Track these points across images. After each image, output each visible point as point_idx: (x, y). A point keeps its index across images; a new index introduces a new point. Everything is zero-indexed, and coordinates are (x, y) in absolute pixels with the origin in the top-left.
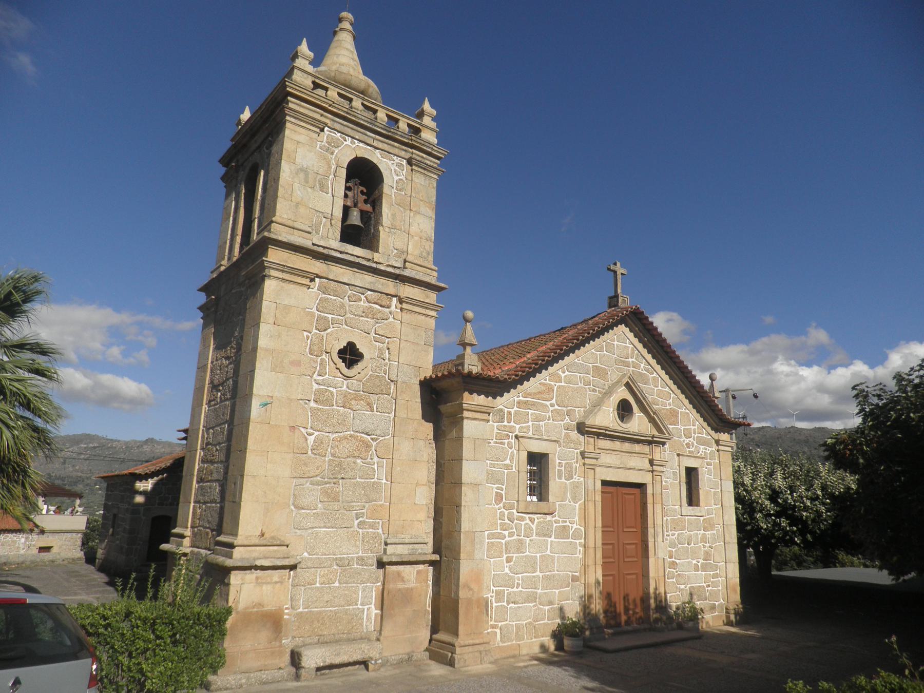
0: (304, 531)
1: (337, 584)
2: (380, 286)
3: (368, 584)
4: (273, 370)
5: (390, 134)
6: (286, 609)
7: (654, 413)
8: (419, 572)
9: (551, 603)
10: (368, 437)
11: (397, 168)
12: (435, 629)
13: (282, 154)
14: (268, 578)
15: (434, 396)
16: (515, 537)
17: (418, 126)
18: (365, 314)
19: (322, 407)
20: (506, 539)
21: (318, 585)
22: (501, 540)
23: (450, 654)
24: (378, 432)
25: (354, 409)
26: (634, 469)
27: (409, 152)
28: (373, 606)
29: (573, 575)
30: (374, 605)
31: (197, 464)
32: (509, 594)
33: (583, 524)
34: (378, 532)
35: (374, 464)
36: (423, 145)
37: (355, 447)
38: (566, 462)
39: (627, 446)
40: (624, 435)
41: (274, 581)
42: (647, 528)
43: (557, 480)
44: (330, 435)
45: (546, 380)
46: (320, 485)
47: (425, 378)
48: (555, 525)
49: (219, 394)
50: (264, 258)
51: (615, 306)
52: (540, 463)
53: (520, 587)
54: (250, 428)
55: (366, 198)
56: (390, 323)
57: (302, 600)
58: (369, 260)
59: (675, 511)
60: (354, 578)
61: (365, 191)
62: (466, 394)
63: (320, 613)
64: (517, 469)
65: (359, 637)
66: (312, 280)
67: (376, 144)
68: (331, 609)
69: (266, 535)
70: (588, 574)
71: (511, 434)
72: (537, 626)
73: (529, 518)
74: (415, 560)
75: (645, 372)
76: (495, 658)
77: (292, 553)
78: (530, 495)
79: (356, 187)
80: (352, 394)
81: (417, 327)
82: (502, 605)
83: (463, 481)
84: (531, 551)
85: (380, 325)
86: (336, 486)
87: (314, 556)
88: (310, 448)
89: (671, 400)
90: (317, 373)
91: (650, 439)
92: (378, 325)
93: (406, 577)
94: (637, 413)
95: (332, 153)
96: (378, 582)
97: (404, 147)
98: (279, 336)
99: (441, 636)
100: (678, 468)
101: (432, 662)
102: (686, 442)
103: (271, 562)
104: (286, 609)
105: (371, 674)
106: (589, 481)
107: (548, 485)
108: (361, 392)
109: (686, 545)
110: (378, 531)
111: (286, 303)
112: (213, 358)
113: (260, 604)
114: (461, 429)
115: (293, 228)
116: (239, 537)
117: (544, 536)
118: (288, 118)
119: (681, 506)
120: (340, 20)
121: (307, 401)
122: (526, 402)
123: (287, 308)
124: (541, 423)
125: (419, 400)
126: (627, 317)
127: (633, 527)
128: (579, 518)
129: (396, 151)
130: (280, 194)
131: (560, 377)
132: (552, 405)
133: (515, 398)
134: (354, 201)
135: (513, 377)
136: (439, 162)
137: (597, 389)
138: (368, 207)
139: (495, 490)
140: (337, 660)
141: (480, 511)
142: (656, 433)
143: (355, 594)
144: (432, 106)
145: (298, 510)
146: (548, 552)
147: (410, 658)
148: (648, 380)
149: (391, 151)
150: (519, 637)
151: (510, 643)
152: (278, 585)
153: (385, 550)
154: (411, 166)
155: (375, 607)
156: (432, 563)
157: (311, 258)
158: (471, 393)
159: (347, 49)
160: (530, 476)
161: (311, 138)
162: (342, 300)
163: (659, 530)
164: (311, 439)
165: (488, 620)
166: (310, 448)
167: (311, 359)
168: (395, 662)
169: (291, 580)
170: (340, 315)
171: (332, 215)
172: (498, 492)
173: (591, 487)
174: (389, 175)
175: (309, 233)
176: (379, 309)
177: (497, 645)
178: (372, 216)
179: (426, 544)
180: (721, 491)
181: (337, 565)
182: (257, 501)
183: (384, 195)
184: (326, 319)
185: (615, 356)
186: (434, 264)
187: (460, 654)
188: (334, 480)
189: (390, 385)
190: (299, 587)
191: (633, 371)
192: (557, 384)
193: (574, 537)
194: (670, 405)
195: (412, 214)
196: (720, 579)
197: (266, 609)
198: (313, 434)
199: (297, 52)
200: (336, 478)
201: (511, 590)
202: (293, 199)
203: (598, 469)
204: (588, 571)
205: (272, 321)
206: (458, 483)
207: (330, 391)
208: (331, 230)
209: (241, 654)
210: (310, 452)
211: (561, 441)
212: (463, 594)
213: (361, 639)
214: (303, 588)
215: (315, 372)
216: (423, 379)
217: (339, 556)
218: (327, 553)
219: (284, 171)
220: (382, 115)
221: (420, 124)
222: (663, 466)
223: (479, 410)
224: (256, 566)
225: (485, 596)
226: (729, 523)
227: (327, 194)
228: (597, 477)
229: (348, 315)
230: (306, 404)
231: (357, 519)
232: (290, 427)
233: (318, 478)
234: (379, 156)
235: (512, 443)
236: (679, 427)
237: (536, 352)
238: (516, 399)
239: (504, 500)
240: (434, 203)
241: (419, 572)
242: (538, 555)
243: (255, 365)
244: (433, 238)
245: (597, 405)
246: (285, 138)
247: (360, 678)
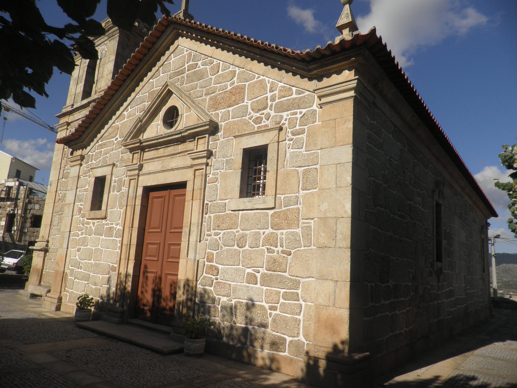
9: (95, 284)
16: (84, 236)
21: (53, 260)
22: (76, 237)
26: (173, 169)
29: (112, 266)
40: (159, 141)
45: (120, 124)
48: (105, 227)
75: (202, 67)
109: (236, 247)
117: (98, 235)
146: (99, 247)
151: (71, 304)
157: (68, 116)
192: (121, 122)
196: (301, 302)
201: (77, 270)
214: (49, 261)
223: (76, 159)
233: (60, 212)
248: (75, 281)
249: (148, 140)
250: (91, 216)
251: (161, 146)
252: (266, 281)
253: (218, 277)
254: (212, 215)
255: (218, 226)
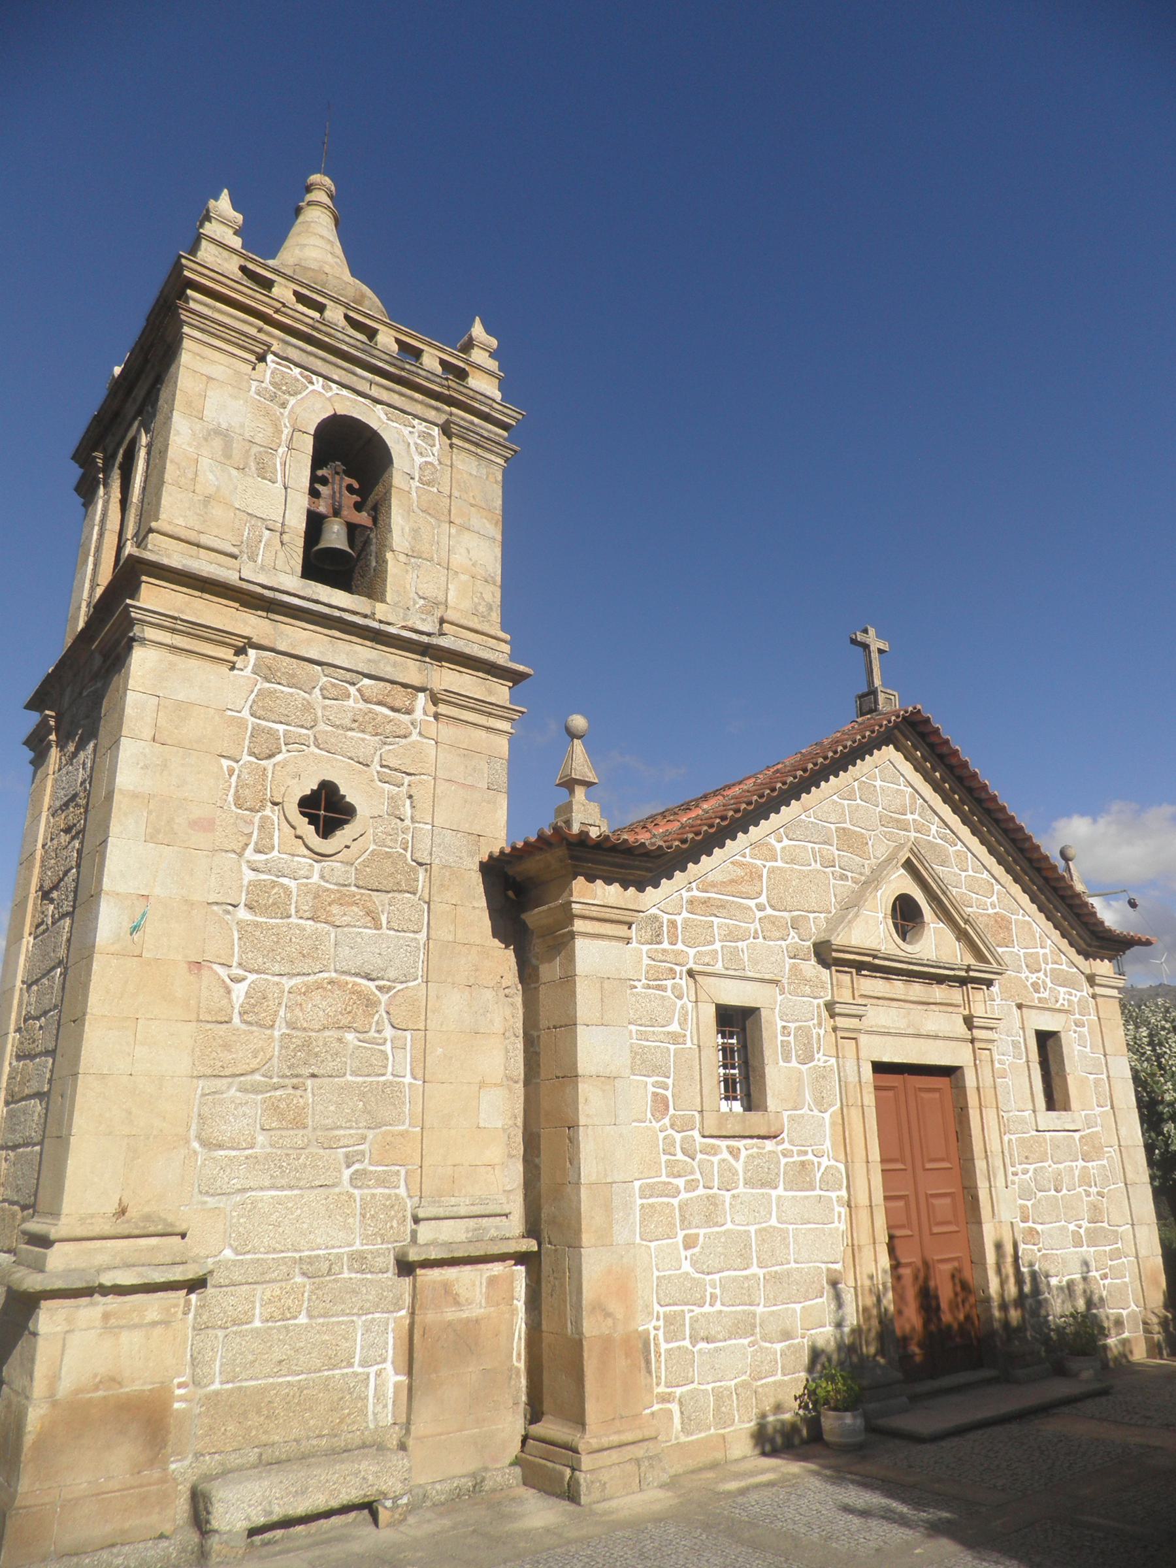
0: (224, 1198)
1: (303, 1320)
2: (389, 669)
3: (377, 1315)
4: (151, 838)
5: (403, 374)
6: (180, 1386)
7: (967, 921)
8: (492, 1281)
9: (787, 1335)
10: (372, 985)
11: (419, 442)
12: (535, 1414)
13: (173, 400)
14: (135, 1314)
15: (510, 893)
16: (701, 1191)
17: (461, 365)
18: (359, 723)
19: (264, 920)
20: (680, 1197)
23: (568, 1472)
24: (392, 974)
25: (337, 923)
26: (936, 1037)
27: (444, 412)
28: (388, 1366)
29: (828, 1270)
30: (393, 1363)
31: (7, 1063)
32: (695, 1320)
33: (842, 1157)
34: (396, 1195)
35: (384, 1043)
36: (472, 398)
37: (340, 1006)
38: (797, 1024)
39: (917, 990)
41: (148, 1319)
42: (973, 1159)
43: (781, 1063)
44: (284, 980)
46: (262, 1092)
47: (491, 856)
48: (783, 1161)
49: (51, 907)
50: (128, 601)
51: (871, 711)
52: (744, 1029)
53: (718, 1302)
54: (95, 967)
55: (359, 499)
56: (413, 745)
57: (218, 1363)
58: (366, 616)
59: (1023, 1121)
60: (344, 1303)
61: (356, 485)
62: (579, 883)
63: (263, 1390)
64: (695, 1042)
65: (358, 1442)
66: (240, 651)
67: (375, 392)
68: (289, 1379)
69: (132, 1213)
70: (861, 1266)
71: (678, 968)
72: (760, 1390)
73: (728, 1147)
74: (482, 1253)
75: (939, 841)
76: (672, 1472)
77: (196, 1250)
78: (727, 1098)
79: (337, 477)
80: (332, 891)
81: (469, 753)
82: (679, 1348)
83: (580, 1071)
84: (736, 1219)
85: (391, 747)
86: (299, 1092)
87: (248, 1257)
88: (236, 1011)
89: (995, 898)
90: (251, 847)
91: (963, 974)
92: (387, 747)
93: (461, 1290)
94: (934, 927)
95: (283, 405)
96: (400, 1310)
97: (433, 402)
98: (165, 765)
99: (549, 1428)
100: (1021, 1032)
101: (529, 1493)
102: (1031, 981)
103: (140, 1275)
104: (180, 1386)
105: (385, 1535)
106: (848, 1064)
107: (763, 1076)
108: (353, 889)
109: (1053, 1192)
110: (397, 1191)
111: (180, 697)
112: (45, 838)
113: (113, 1379)
114: (571, 959)
115: (198, 546)
116: (63, 1220)
117: (763, 1185)
118: (186, 329)
119: (1034, 1111)
120: (309, 189)
121: (230, 908)
122: (705, 902)
123: (182, 708)
124: (740, 944)
125: (483, 903)
126: (896, 731)
127: (942, 1160)
128: (833, 1145)
129: (418, 409)
130: (168, 477)
131: (772, 849)
132: (761, 908)
133: (683, 891)
134: (333, 505)
135: (677, 843)
136: (505, 434)
137: (849, 874)
138: (363, 518)
139: (651, 1089)
140: (301, 1508)
141: (621, 1135)
142: (970, 960)
143: (347, 1340)
144: (488, 331)
145: (210, 1150)
146: (774, 1222)
147: (477, 1486)
148: (948, 856)
149: (407, 408)
150: (723, 1419)
151: (703, 1435)
152: (159, 1330)
153: (414, 1234)
154: (449, 438)
155: (395, 1369)
156: (521, 1258)
157: (237, 605)
158: (591, 879)
159: (322, 237)
160: (724, 1057)
161: (237, 372)
162: (306, 695)
163: (997, 1164)
164: (239, 991)
165: (651, 1385)
166: (236, 1011)
167: (238, 816)
168: (443, 1498)
169: (191, 1316)
170: (302, 726)
171: (283, 524)
172: (658, 1094)
173: (852, 1078)
174: (404, 453)
175: (235, 557)
176: (386, 716)
177: (674, 1442)
178: (372, 535)
179: (506, 1215)
180: (1108, 1077)
181: (304, 1274)
182: (110, 1134)
183: (394, 491)
184: (271, 733)
185: (880, 809)
186: (503, 629)
187: (592, 1471)
188: (295, 1081)
189: (416, 872)
190: (210, 1331)
191: (916, 838)
192: (768, 864)
193: (827, 1185)
194: (993, 906)
195: (453, 531)
197: (127, 1390)
198: (244, 979)
199: (208, 211)
200: (297, 1076)
201: (697, 1310)
202: (198, 488)
203: (863, 1039)
204: (861, 1258)
205: (147, 733)
206: (570, 1077)
207: (282, 885)
208: (281, 554)
209: (62, 1507)
210: (236, 1019)
211: (785, 981)
212: (591, 1327)
213: (364, 1446)
214: (220, 1334)
215: (247, 845)
216: (485, 858)
217: (307, 1253)
218: (279, 1247)
219: (178, 433)
220: (386, 339)
221: (466, 361)
222: (991, 1029)
223: (607, 916)
224: (101, 1286)
225: (641, 1329)
226: (1130, 1143)
227: (273, 483)
228: (862, 1055)
229: (322, 726)
230: (228, 912)
231: (348, 1167)
232: (190, 963)
233: (257, 1077)
234: (384, 417)
235: (681, 988)
236: (1015, 950)
237: (720, 798)
238: (686, 895)
239: (671, 1111)
240: (499, 512)
241: (492, 1281)
242: (752, 1229)
243: (108, 827)
244: (499, 579)
245: (852, 905)
246: (181, 368)
247: (356, 1547)
248: (695, 1350)
249: (894, 957)
250: (729, 1126)
251: (898, 975)
252: (1094, 1238)
253: (1041, 1245)
254: (1013, 1137)
255: (1027, 1158)
